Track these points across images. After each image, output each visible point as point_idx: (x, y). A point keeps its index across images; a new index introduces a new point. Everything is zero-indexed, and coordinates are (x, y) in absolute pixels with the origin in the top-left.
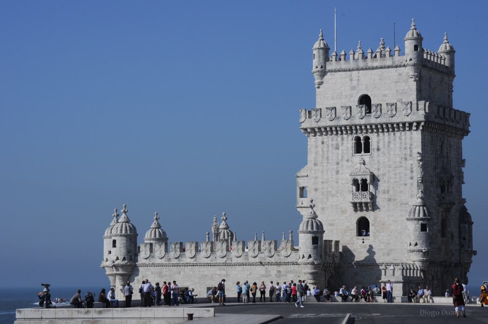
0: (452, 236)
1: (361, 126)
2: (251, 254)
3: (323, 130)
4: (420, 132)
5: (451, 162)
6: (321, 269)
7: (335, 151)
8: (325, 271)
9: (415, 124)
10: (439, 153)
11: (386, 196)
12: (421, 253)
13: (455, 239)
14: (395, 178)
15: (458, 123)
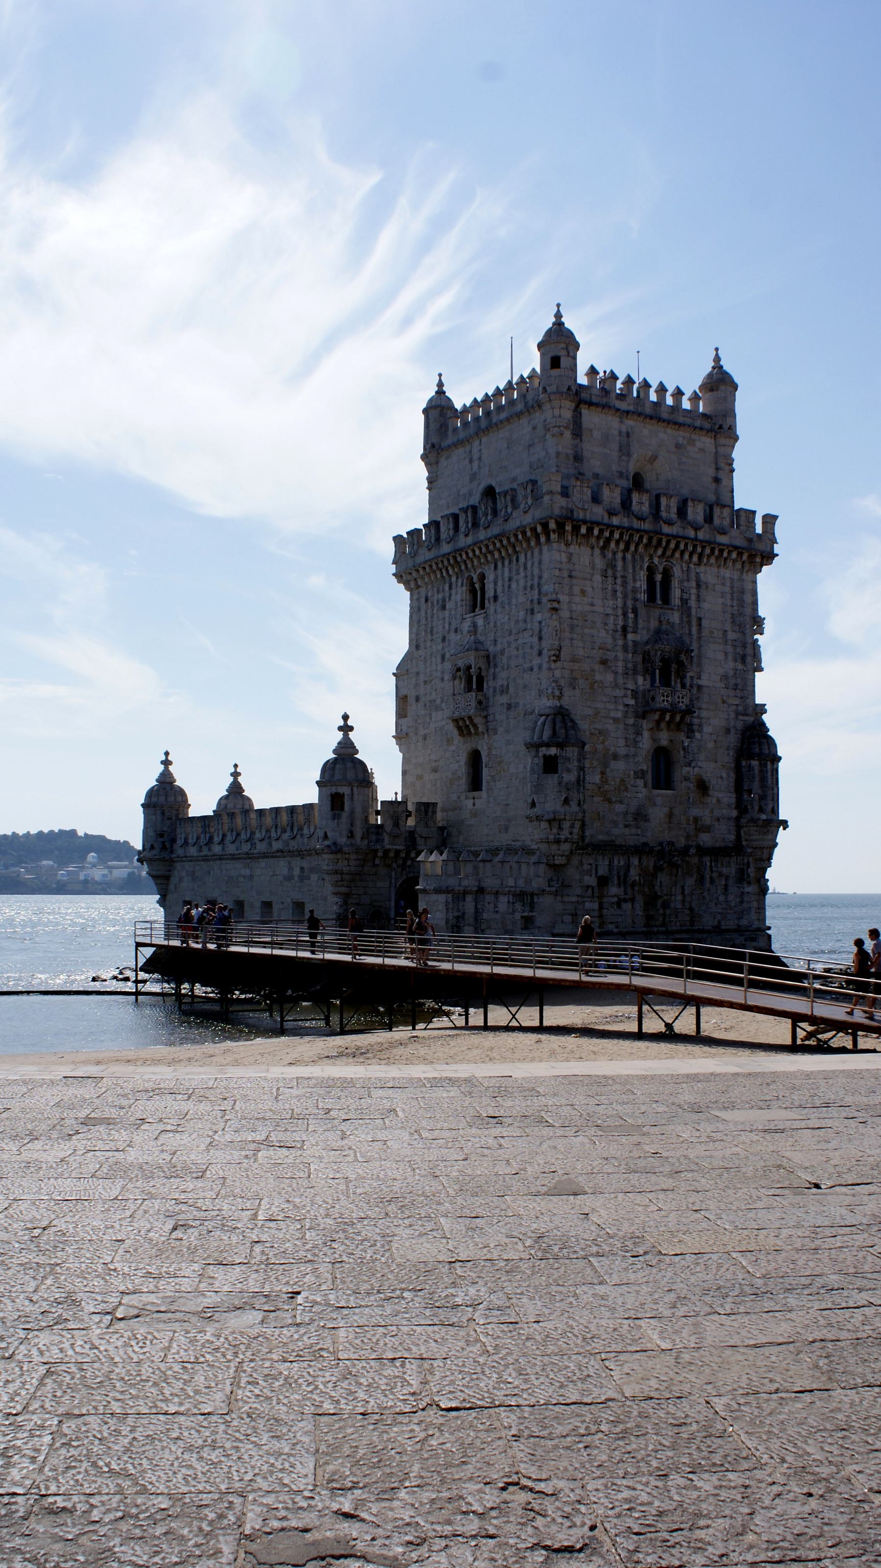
0: (703, 787)
1: (467, 554)
2: (273, 834)
3: (421, 572)
4: (555, 545)
5: (705, 623)
6: (352, 863)
7: (440, 613)
8: (389, 866)
9: (539, 529)
10: (643, 597)
11: (504, 699)
12: (544, 825)
13: (710, 793)
14: (517, 656)
15: (724, 533)
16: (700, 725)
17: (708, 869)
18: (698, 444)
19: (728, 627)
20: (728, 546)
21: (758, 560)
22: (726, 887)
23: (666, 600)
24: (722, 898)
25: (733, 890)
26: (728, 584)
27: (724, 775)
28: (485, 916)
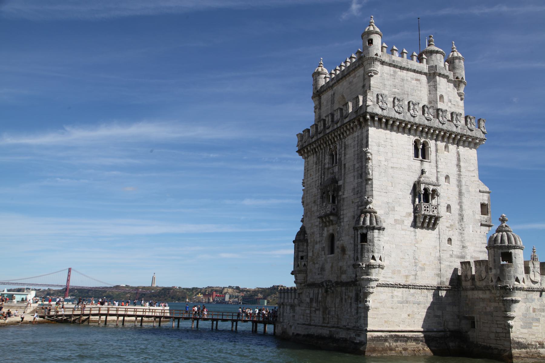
0: (343, 250)
13: (346, 253)
15: (347, 117)
16: (343, 218)
17: (344, 295)
18: (357, 75)
19: (355, 163)
20: (346, 123)
21: (361, 120)
22: (351, 303)
23: (336, 163)
24: (349, 310)
25: (354, 305)
26: (356, 139)
27: (352, 242)
28: (285, 314)
